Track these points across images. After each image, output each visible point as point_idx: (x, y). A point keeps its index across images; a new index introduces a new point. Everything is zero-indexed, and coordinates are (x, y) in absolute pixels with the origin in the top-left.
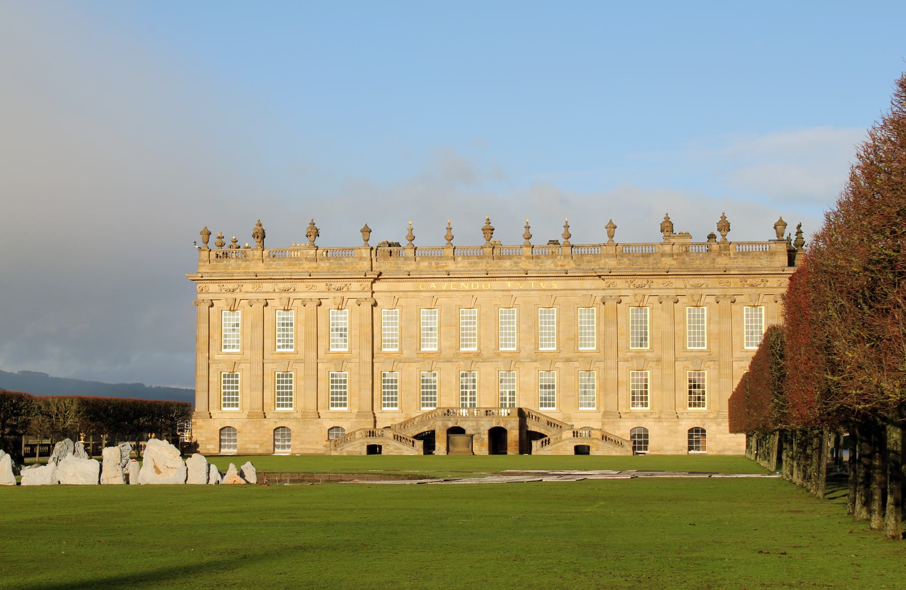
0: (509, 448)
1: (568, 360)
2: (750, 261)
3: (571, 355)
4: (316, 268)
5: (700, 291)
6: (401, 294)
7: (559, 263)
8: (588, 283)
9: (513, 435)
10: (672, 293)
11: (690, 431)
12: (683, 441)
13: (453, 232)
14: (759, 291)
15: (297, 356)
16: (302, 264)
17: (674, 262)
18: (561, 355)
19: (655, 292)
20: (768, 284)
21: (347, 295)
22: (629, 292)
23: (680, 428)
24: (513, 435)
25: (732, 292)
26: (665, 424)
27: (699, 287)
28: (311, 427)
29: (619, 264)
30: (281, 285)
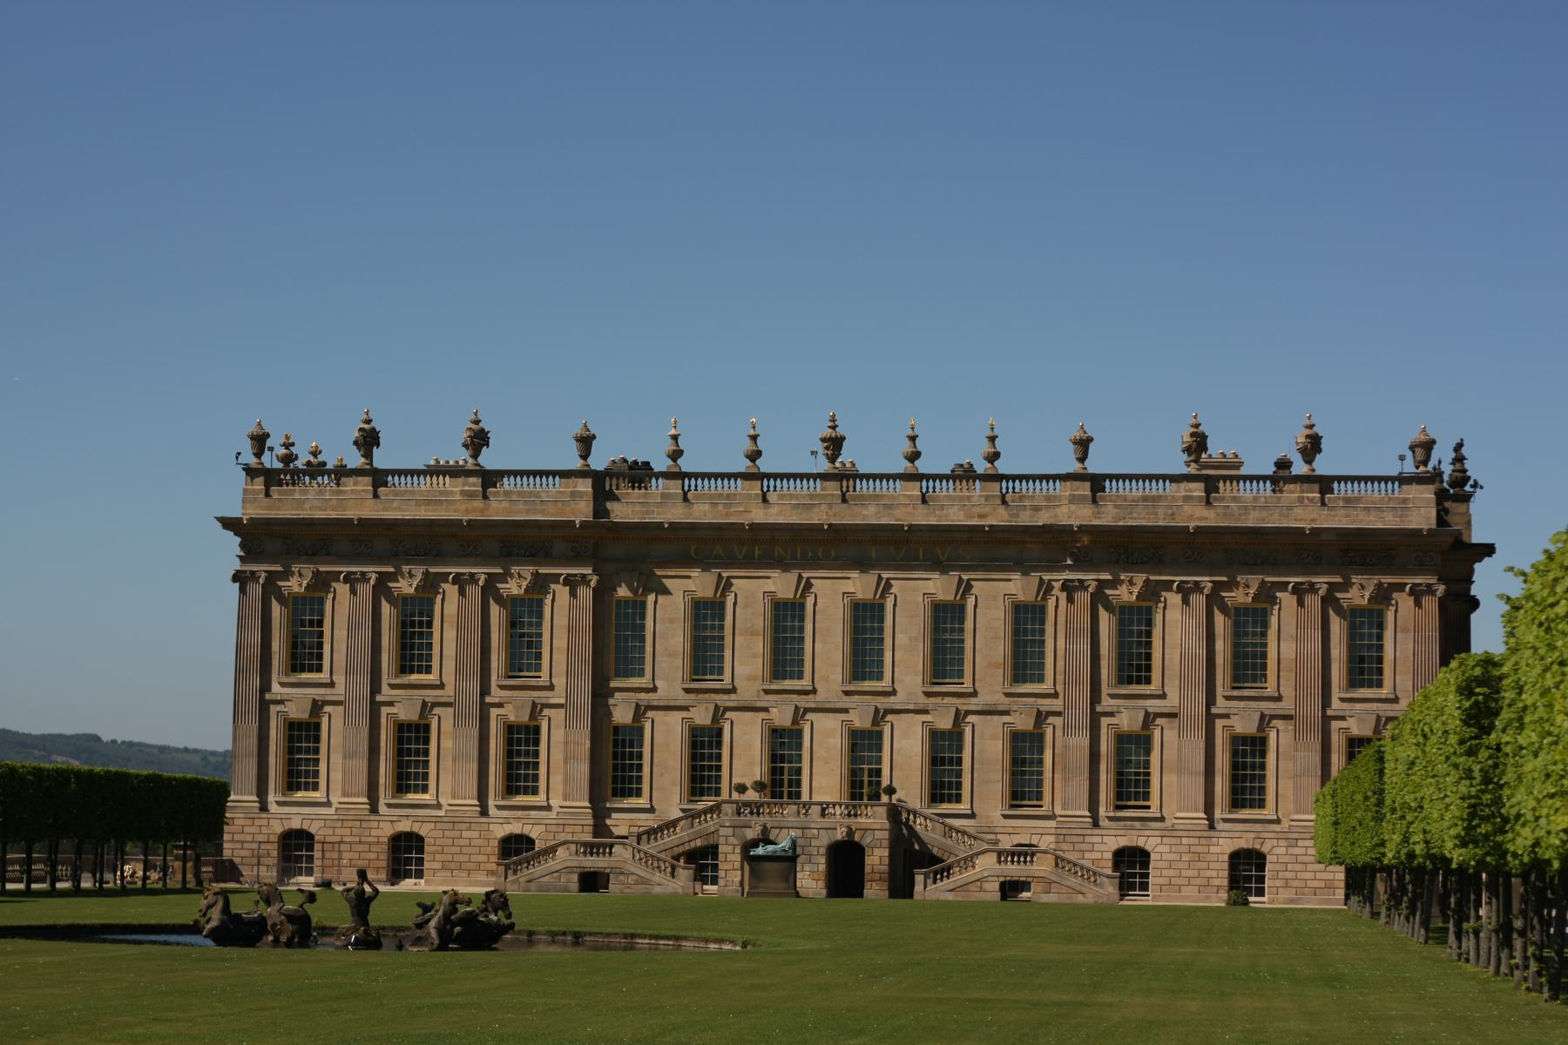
2: (1362, 515)
4: (482, 511)
9: (877, 858)
13: (762, 444)
23: (1213, 849)
24: (877, 858)
26: (1185, 841)
29: (1096, 515)
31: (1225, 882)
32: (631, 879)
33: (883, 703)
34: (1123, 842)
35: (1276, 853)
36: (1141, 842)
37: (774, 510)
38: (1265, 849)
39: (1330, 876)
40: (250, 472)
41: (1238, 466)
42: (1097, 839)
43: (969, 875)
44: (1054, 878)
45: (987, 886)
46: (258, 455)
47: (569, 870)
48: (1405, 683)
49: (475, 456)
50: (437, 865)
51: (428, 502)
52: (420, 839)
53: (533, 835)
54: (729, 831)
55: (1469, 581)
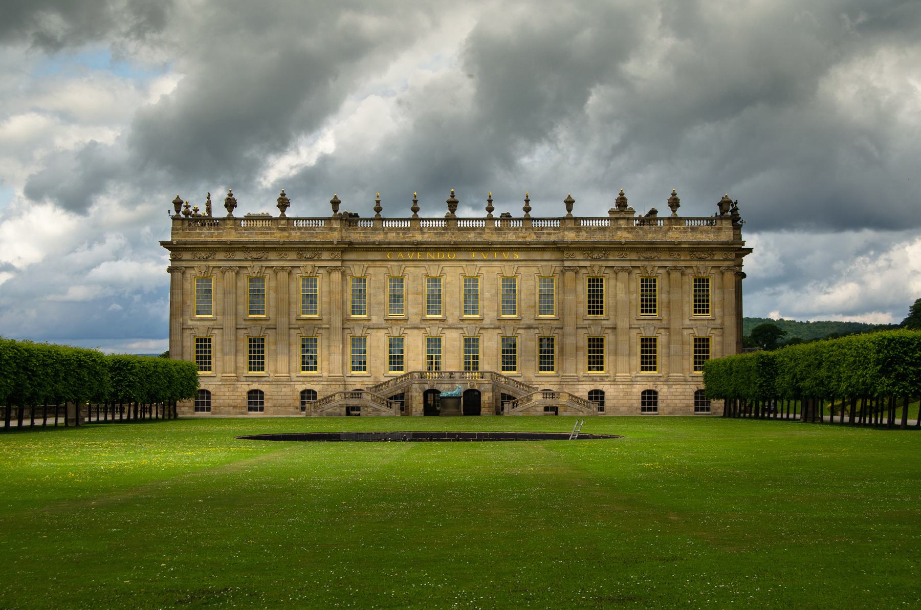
0: (482, 409)
1: (529, 327)
2: (699, 236)
3: (532, 322)
4: (288, 237)
5: (653, 263)
6: (370, 263)
7: (521, 235)
8: (547, 256)
10: (626, 264)
11: (643, 393)
12: (637, 401)
14: (707, 263)
15: (268, 323)
16: (273, 233)
17: (628, 235)
18: (522, 322)
19: (611, 264)
20: (716, 258)
21: (318, 264)
22: (587, 264)
23: (634, 390)
24: (486, 397)
25: (682, 264)
27: (652, 259)
28: (283, 390)
29: (577, 236)
30: (254, 255)
31: (640, 405)
32: (370, 410)
33: (479, 324)
34: (593, 388)
35: (663, 391)
36: (600, 387)
37: (426, 236)
38: (657, 390)
39: (686, 401)
40: (174, 219)
41: (634, 212)
42: (580, 387)
43: (529, 404)
44: (569, 404)
45: (538, 409)
46: (178, 211)
47: (342, 406)
48: (718, 311)
49: (230, 211)
50: (269, 405)
51: (262, 233)
52: (262, 393)
53: (316, 390)
54: (417, 386)
55: (741, 265)
